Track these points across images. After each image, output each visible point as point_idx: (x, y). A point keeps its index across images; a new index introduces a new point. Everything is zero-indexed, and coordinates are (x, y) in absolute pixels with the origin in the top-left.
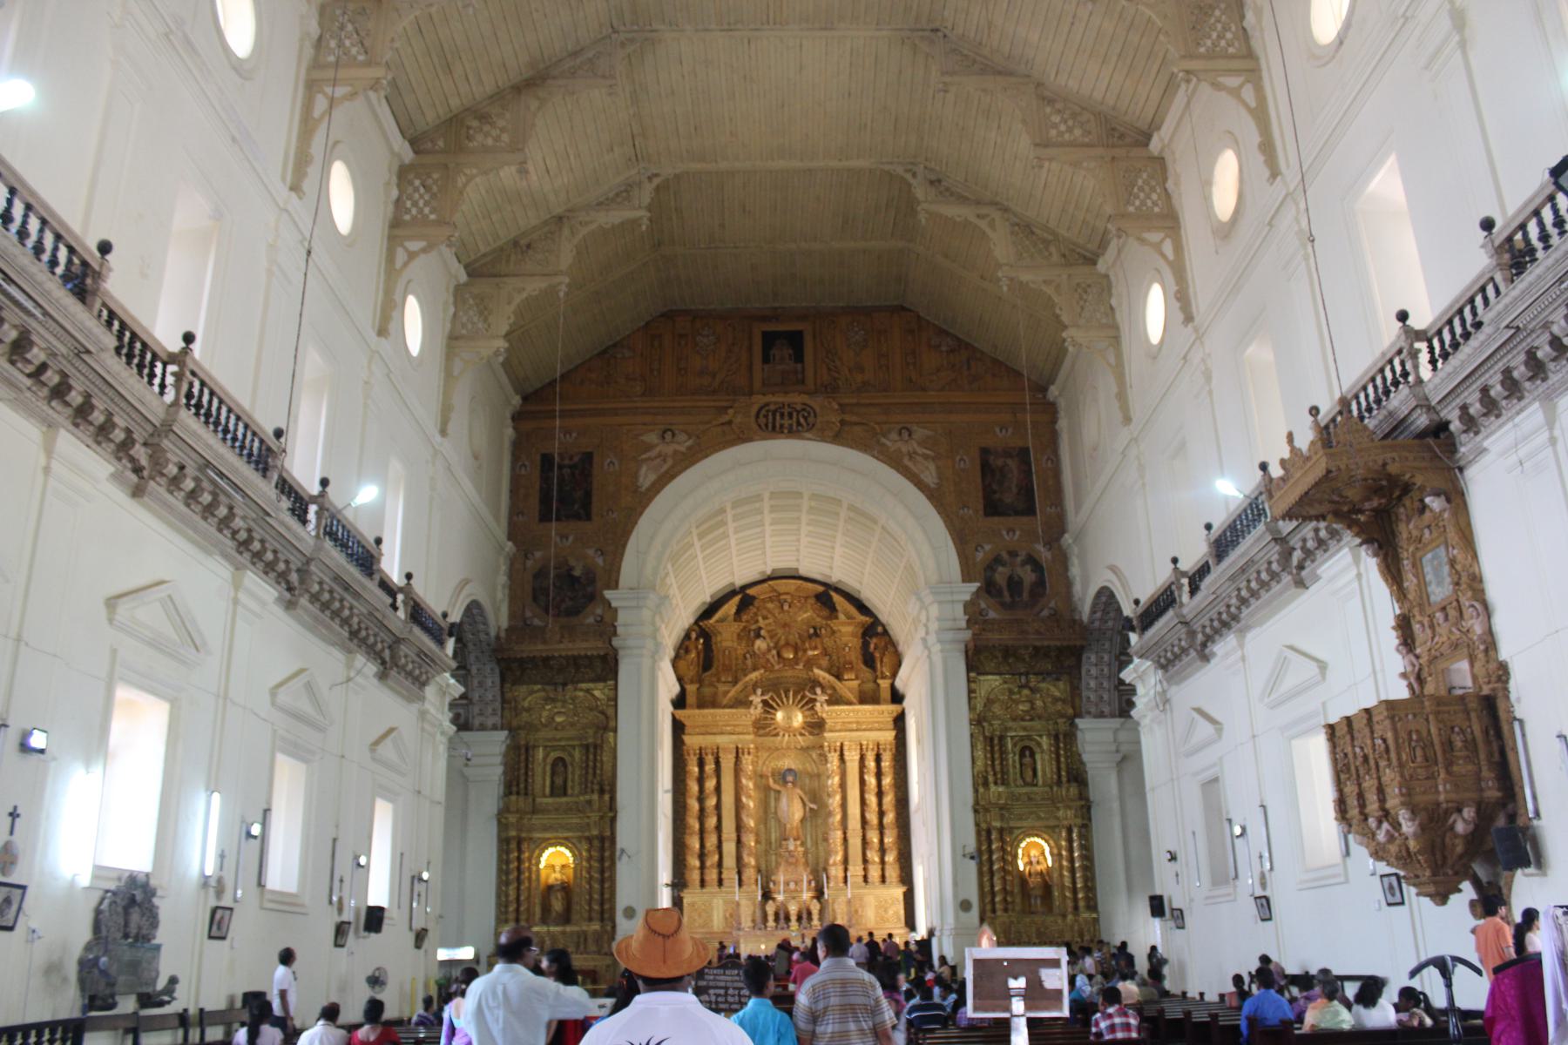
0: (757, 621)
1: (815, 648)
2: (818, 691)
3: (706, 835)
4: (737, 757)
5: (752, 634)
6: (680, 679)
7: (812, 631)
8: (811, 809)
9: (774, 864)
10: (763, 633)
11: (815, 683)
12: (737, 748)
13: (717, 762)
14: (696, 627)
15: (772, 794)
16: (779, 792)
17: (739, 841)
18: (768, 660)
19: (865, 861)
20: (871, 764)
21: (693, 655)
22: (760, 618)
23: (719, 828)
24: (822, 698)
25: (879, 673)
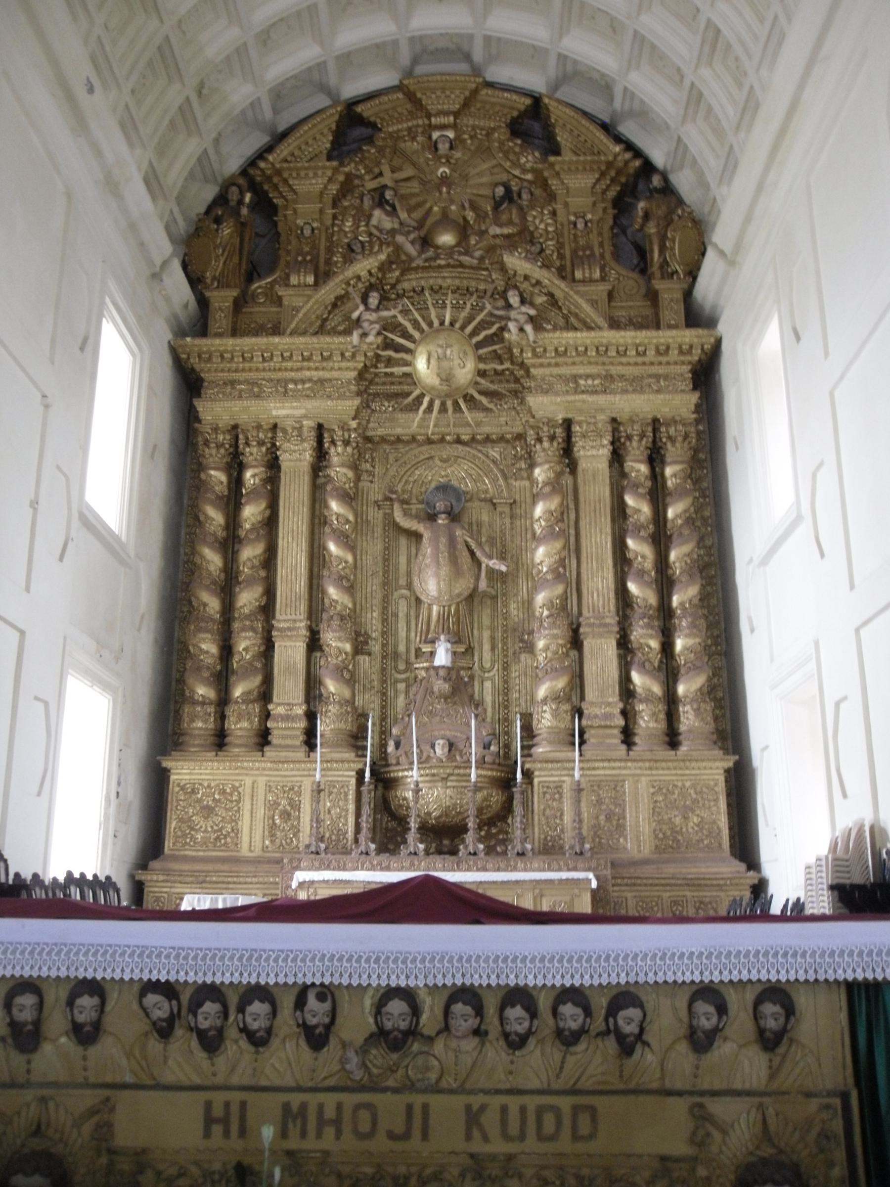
0: (381, 174)
1: (510, 223)
2: (514, 300)
3: (236, 625)
4: (321, 454)
5: (367, 202)
6: (195, 281)
7: (500, 191)
8: (491, 572)
9: (401, 701)
10: (388, 195)
11: (511, 282)
12: (320, 427)
13: (273, 465)
14: (241, 181)
15: (403, 541)
16: (417, 537)
17: (314, 644)
18: (398, 248)
19: (627, 692)
20: (638, 469)
21: (227, 231)
22: (386, 169)
23: (267, 609)
24: (520, 313)
25: (655, 269)
